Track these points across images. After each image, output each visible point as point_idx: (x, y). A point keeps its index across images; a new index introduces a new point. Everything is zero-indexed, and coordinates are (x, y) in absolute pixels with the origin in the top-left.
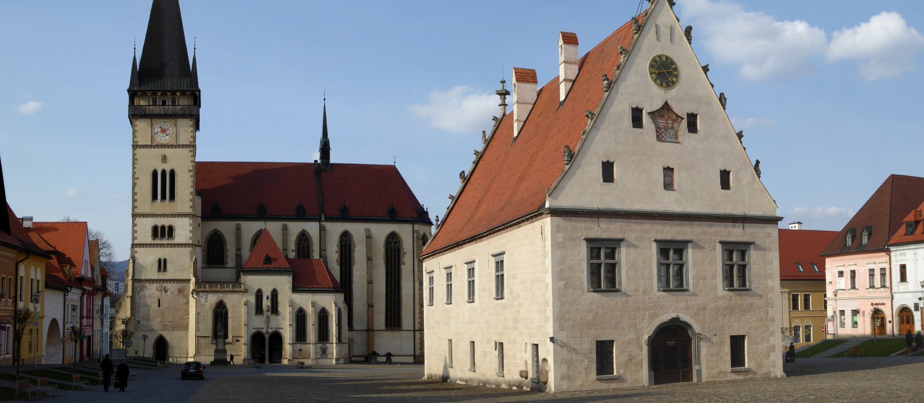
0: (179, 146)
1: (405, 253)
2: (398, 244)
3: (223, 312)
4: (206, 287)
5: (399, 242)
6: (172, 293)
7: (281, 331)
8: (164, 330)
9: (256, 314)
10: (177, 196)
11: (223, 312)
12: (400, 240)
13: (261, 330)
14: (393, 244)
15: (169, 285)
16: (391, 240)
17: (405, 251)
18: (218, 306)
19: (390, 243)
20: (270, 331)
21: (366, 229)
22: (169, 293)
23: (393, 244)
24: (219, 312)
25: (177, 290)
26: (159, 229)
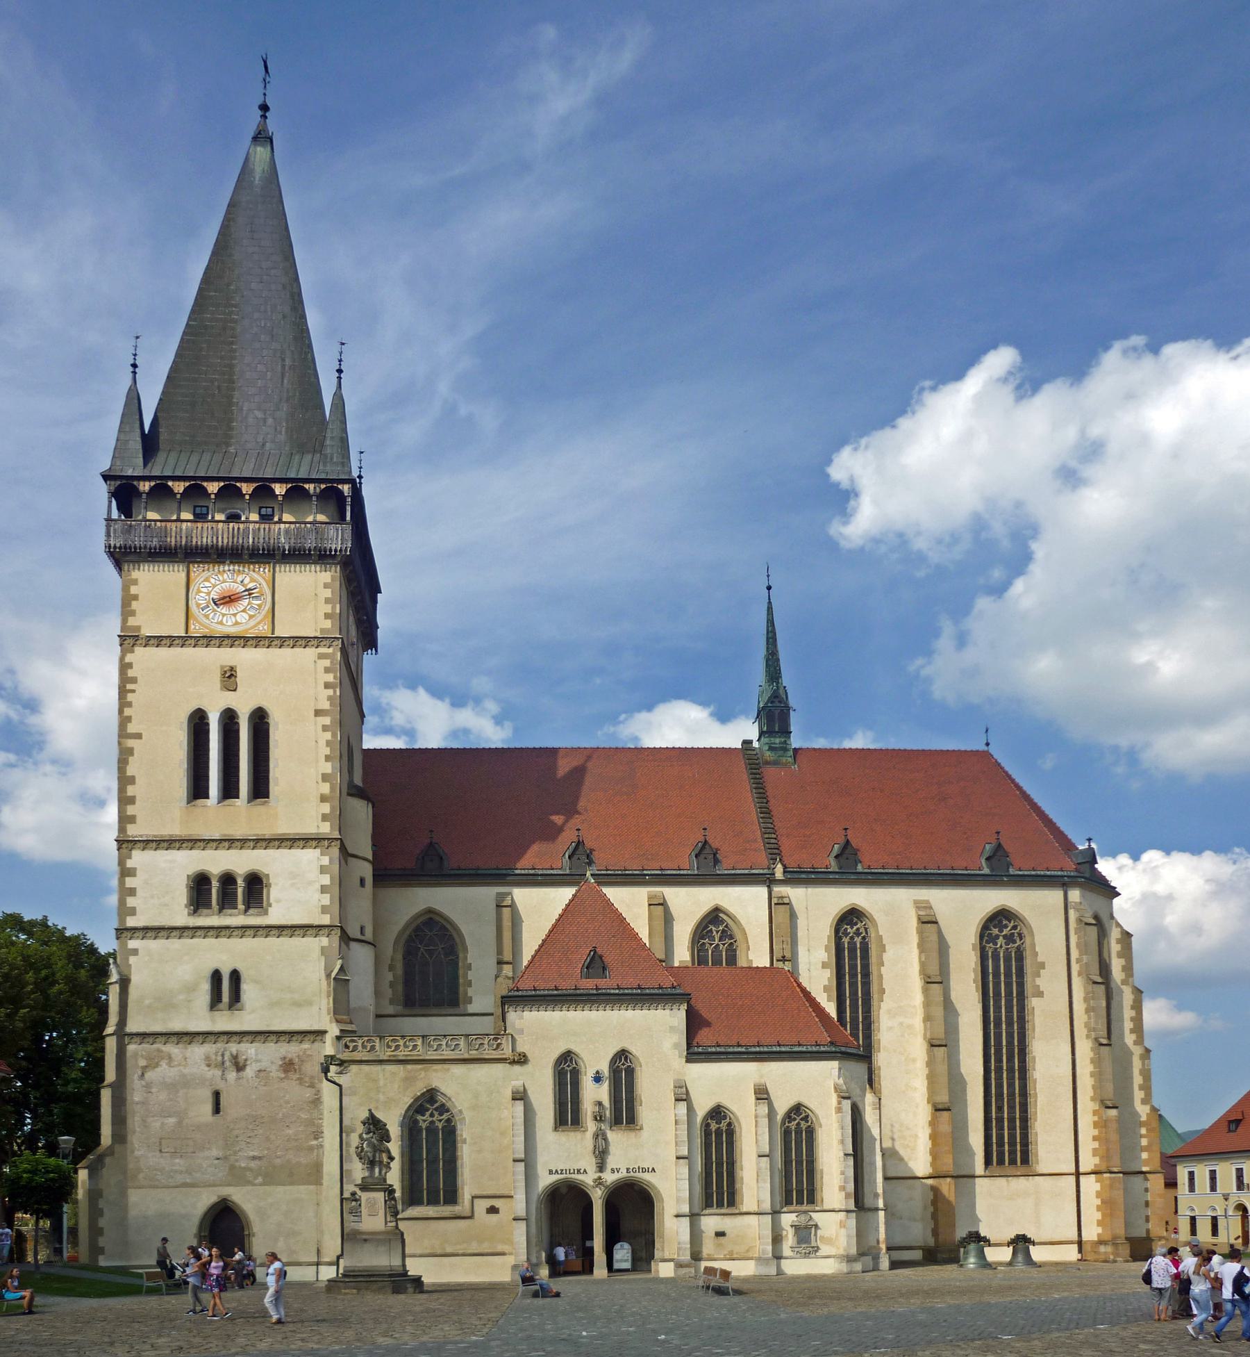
0: (283, 642)
1: (1042, 965)
2: (1018, 943)
3: (440, 1125)
4: (373, 1048)
5: (1021, 936)
6: (259, 1071)
7: (647, 1177)
8: (237, 1176)
9: (556, 1129)
10: (277, 785)
11: (440, 1125)
12: (1025, 932)
13: (573, 1176)
14: (1001, 941)
15: (249, 1050)
16: (995, 931)
17: (1040, 959)
18: (421, 1105)
19: (993, 939)
20: (610, 1178)
21: (916, 902)
22: (249, 1072)
23: (1001, 941)
24: (424, 1125)
25: (281, 1063)
26: (215, 884)
